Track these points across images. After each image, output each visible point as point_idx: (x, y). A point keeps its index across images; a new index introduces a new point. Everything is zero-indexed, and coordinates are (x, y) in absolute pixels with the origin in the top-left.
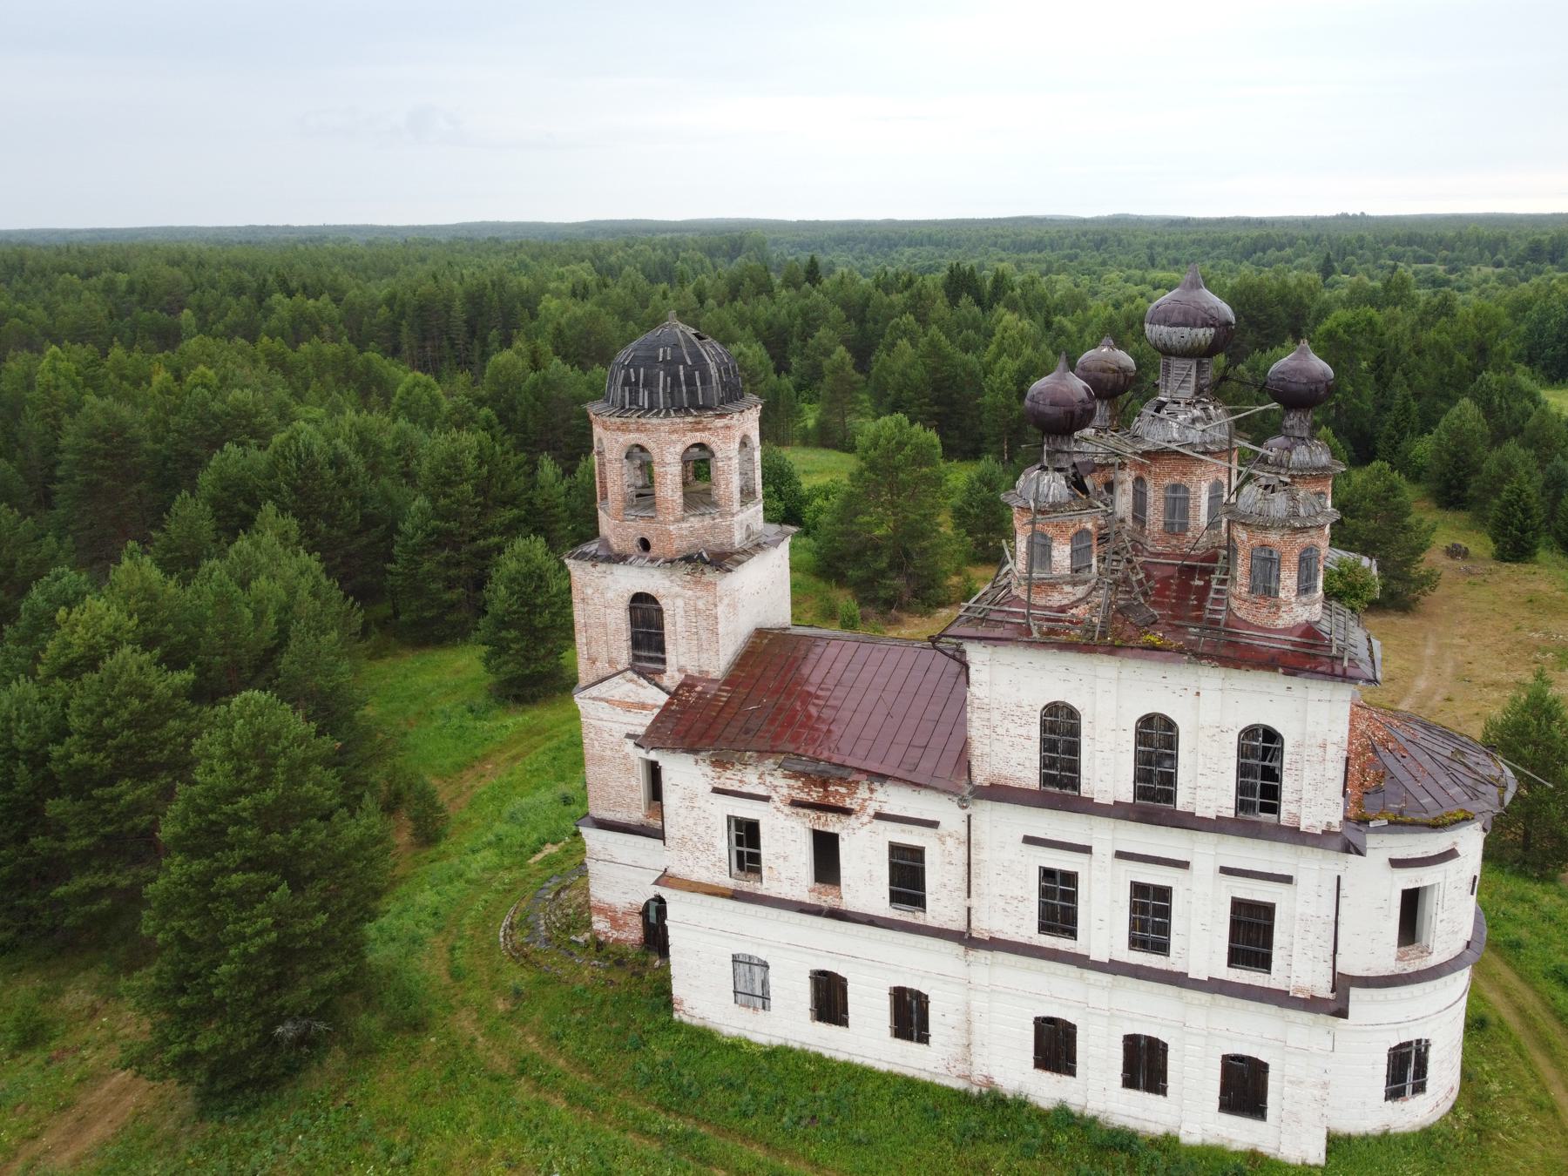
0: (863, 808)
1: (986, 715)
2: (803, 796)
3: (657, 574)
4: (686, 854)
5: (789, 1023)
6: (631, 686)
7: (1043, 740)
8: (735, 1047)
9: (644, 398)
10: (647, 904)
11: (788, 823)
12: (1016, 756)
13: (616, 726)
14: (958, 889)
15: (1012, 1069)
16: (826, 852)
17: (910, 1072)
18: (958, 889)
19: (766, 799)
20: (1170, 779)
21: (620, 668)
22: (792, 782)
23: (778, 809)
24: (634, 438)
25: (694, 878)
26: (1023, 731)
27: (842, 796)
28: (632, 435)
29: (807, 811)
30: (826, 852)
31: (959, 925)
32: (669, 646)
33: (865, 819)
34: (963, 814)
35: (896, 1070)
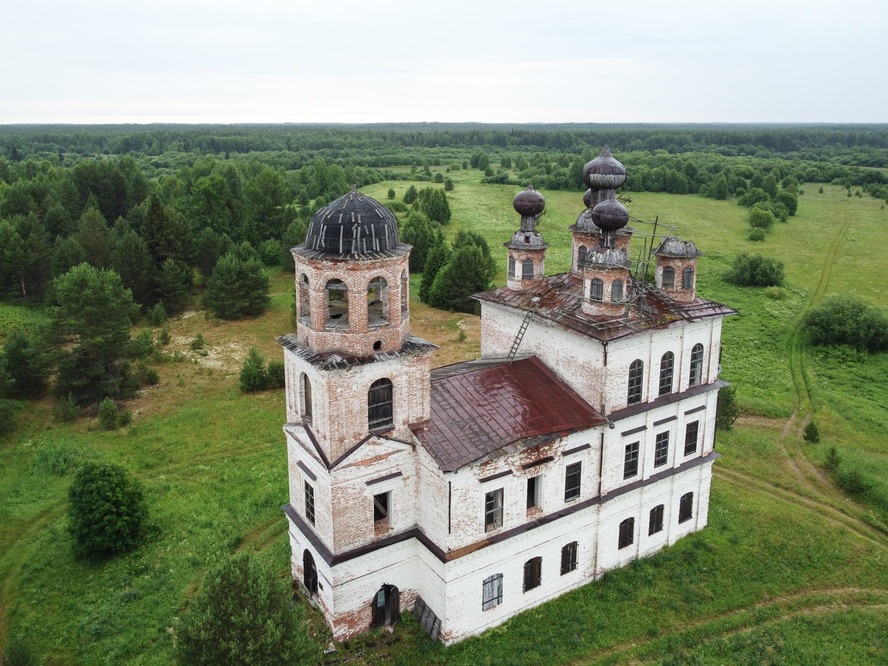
2: (528, 461)
5: (517, 601)
6: (371, 447)
8: (494, 635)
9: (376, 244)
10: (376, 596)
13: (359, 480)
17: (568, 590)
19: (510, 472)
21: (362, 437)
24: (375, 273)
25: (464, 545)
28: (376, 271)
35: (562, 592)
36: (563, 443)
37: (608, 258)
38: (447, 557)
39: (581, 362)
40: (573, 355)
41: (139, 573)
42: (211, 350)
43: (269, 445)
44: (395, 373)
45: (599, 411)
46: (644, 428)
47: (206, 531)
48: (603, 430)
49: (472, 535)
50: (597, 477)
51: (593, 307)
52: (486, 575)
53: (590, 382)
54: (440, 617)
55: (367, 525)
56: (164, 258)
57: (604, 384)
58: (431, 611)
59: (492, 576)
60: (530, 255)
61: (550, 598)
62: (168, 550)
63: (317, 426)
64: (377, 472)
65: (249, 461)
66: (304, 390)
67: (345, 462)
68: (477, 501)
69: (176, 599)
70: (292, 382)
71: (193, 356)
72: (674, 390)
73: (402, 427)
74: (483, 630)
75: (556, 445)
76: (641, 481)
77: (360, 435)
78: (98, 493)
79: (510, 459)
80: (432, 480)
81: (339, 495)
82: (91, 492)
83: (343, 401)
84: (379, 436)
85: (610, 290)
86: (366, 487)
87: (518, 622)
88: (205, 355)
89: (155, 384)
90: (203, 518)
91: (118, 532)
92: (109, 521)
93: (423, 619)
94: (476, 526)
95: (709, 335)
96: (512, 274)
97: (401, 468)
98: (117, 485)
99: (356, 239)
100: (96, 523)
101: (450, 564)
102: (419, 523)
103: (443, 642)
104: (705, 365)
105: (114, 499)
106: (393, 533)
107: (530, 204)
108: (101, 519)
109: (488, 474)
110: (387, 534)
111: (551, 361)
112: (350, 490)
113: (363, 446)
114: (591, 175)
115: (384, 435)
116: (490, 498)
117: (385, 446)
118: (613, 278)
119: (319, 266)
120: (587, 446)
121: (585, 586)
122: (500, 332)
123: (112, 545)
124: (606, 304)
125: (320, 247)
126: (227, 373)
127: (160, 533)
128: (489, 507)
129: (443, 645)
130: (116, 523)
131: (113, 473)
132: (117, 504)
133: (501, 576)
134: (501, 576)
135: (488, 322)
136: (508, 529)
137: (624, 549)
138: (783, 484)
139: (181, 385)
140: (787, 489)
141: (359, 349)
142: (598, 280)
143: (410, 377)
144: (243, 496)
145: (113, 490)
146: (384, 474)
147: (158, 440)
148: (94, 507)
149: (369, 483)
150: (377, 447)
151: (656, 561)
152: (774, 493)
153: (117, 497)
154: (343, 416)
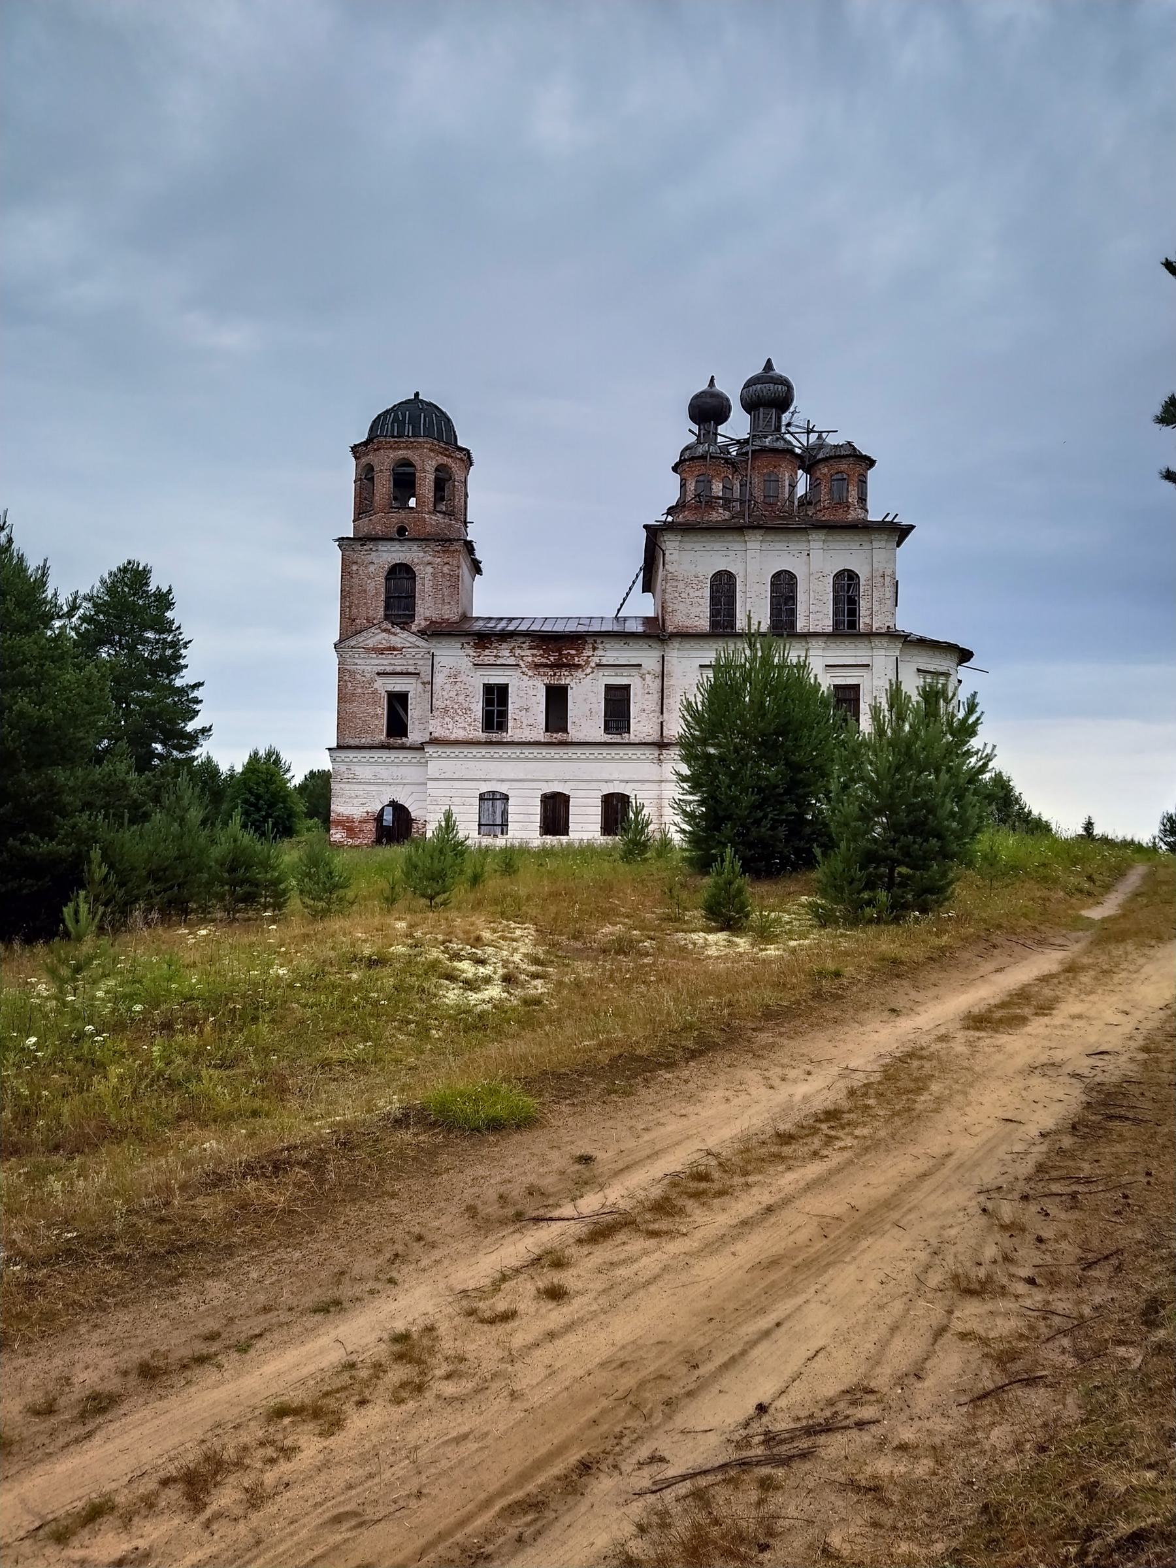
0: (587, 663)
1: (675, 584)
4: (448, 719)
7: (711, 598)
11: (531, 683)
12: (694, 611)
14: (654, 711)
16: (557, 699)
18: (654, 711)
20: (793, 612)
22: (535, 652)
23: (523, 673)
25: (453, 737)
26: (699, 593)
27: (573, 656)
29: (546, 670)
30: (557, 699)
31: (655, 737)
32: (418, 602)
33: (589, 670)
34: (658, 654)
36: (599, 653)
49: (464, 728)
68: (471, 689)
116: (488, 689)
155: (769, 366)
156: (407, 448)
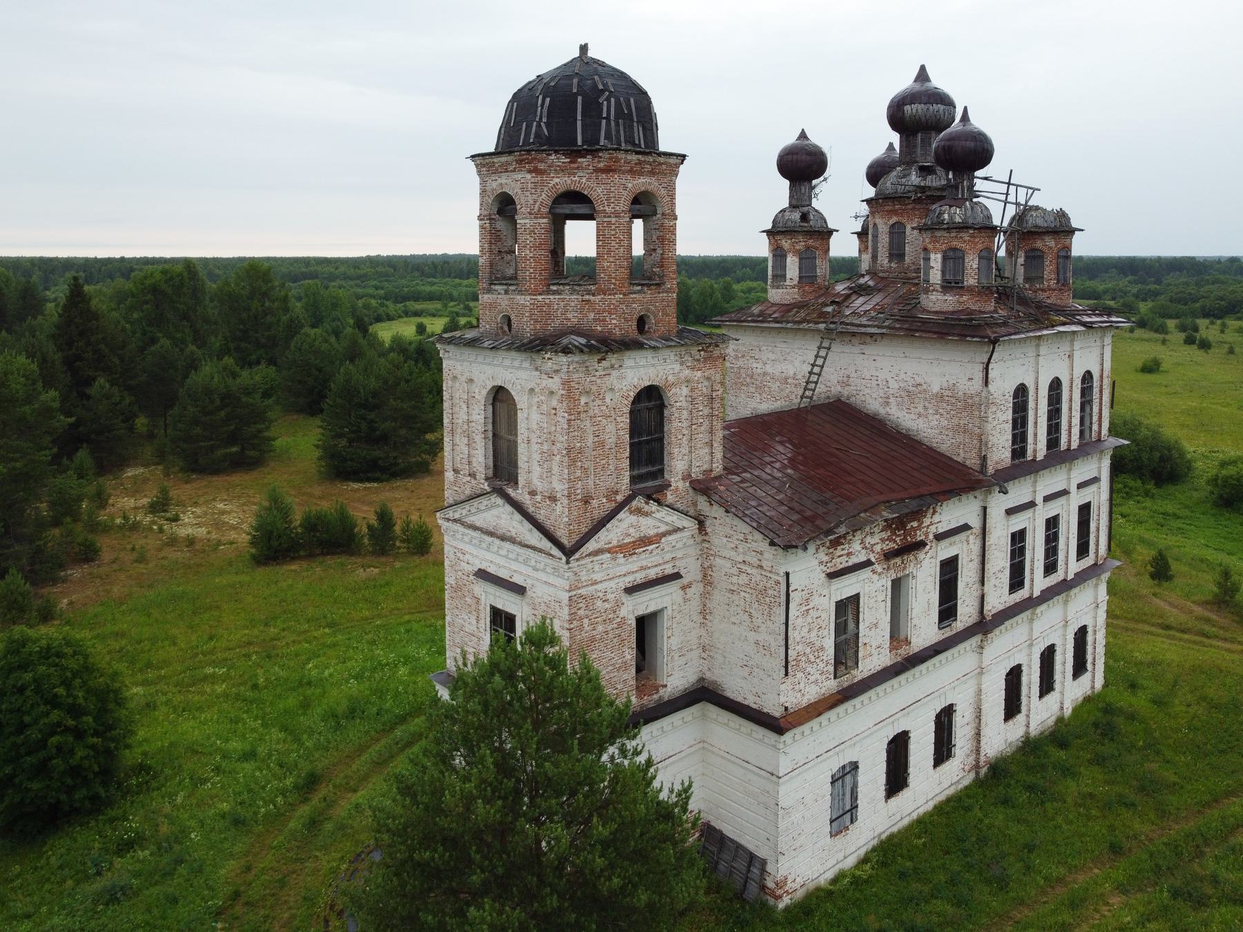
2: (892, 545)
3: (671, 355)
11: (880, 584)
13: (612, 584)
15: (1001, 737)
19: (868, 563)
21: (620, 498)
37: (969, 213)
38: (782, 723)
39: (935, 388)
40: (919, 380)
41: (125, 847)
42: (184, 513)
43: (327, 630)
44: (671, 379)
45: (977, 468)
46: (1032, 504)
47: (248, 766)
48: (984, 500)
49: (816, 682)
50: (977, 586)
51: (949, 297)
52: (835, 764)
53: (956, 421)
54: (761, 853)
55: (625, 676)
56: (89, 382)
57: (984, 419)
58: (739, 847)
59: (844, 767)
60: (810, 242)
61: (921, 811)
62: (179, 800)
63: (529, 483)
64: (643, 568)
65: (297, 655)
66: (490, 427)
67: (592, 545)
69: (211, 889)
70: (462, 416)
71: (154, 523)
72: (1063, 445)
73: (681, 485)
74: (830, 875)
75: (927, 521)
76: (1030, 598)
77: (617, 493)
78: (38, 691)
79: (868, 540)
80: (743, 579)
81: (581, 612)
82: (21, 690)
83: (588, 423)
84: (649, 497)
85: (975, 266)
86: (625, 598)
87: (887, 852)
88: (176, 519)
89: (93, 560)
90: (235, 745)
91: (75, 771)
92: (59, 749)
93: (722, 866)
94: (822, 665)
95: (1098, 359)
96: (780, 276)
97: (681, 566)
98: (75, 675)
99: (608, 118)
100: (29, 753)
101: (788, 736)
102: (708, 675)
103: (771, 901)
104: (1096, 409)
105: (70, 700)
106: (666, 694)
107: (808, 158)
108: (42, 744)
109: (841, 563)
110: (655, 697)
111: (872, 403)
112: (599, 603)
113: (621, 515)
114: (907, 108)
115: (655, 495)
117: (656, 519)
118: (980, 246)
119: (542, 166)
120: (965, 527)
121: (966, 788)
122: (765, 374)
123: (64, 797)
124: (970, 290)
125: (538, 135)
126: (219, 543)
127: (154, 777)
128: (840, 629)
129: (773, 909)
130: (72, 752)
131: (68, 650)
132: (75, 711)
133: (855, 766)
134: (855, 766)
135: (740, 363)
136: (866, 674)
137: (1011, 722)
138: (1173, 624)
139: (141, 559)
140: (1183, 631)
141: (617, 325)
142: (955, 249)
143: (692, 390)
144: (305, 705)
145: (67, 684)
146: (653, 574)
147: (120, 635)
148: (27, 719)
149: (631, 590)
150: (644, 521)
151: (1060, 735)
152: (1168, 637)
153: (76, 697)
154: (589, 453)
155: (922, 75)
156: (652, 173)
